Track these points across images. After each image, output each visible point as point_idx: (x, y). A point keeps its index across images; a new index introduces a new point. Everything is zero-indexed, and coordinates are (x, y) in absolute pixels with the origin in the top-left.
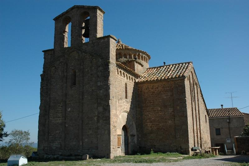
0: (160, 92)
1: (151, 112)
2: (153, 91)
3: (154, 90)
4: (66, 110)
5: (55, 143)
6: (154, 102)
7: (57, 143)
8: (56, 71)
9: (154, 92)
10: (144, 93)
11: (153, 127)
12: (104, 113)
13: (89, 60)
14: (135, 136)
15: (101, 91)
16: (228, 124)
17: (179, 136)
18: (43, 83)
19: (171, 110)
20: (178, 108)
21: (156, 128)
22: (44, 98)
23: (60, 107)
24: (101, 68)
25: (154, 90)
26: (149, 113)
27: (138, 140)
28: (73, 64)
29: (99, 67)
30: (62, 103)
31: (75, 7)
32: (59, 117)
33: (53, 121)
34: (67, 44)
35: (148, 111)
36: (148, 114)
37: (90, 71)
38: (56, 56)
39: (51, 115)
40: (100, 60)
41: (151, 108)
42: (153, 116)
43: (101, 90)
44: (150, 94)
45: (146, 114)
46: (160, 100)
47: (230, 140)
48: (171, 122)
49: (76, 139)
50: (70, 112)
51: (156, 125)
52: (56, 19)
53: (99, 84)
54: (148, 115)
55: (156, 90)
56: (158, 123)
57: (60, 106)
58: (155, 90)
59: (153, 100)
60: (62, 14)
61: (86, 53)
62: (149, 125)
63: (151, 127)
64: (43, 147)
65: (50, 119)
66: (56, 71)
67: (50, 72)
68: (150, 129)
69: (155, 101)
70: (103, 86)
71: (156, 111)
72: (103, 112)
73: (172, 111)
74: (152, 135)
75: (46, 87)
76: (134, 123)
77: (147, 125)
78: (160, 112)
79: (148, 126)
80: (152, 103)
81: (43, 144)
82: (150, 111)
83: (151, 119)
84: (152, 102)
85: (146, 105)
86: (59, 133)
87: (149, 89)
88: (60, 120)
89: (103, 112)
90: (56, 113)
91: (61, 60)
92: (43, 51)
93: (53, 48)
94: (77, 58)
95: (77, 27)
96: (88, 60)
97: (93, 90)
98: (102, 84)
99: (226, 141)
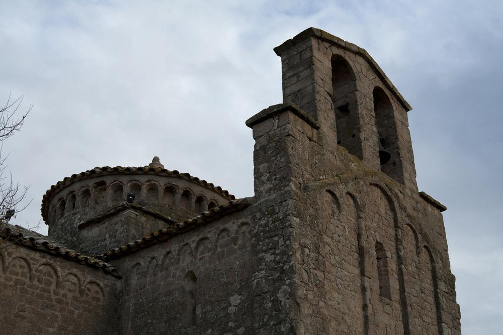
37: (417, 277)
38: (325, 157)
66: (334, 213)
75: (312, 254)
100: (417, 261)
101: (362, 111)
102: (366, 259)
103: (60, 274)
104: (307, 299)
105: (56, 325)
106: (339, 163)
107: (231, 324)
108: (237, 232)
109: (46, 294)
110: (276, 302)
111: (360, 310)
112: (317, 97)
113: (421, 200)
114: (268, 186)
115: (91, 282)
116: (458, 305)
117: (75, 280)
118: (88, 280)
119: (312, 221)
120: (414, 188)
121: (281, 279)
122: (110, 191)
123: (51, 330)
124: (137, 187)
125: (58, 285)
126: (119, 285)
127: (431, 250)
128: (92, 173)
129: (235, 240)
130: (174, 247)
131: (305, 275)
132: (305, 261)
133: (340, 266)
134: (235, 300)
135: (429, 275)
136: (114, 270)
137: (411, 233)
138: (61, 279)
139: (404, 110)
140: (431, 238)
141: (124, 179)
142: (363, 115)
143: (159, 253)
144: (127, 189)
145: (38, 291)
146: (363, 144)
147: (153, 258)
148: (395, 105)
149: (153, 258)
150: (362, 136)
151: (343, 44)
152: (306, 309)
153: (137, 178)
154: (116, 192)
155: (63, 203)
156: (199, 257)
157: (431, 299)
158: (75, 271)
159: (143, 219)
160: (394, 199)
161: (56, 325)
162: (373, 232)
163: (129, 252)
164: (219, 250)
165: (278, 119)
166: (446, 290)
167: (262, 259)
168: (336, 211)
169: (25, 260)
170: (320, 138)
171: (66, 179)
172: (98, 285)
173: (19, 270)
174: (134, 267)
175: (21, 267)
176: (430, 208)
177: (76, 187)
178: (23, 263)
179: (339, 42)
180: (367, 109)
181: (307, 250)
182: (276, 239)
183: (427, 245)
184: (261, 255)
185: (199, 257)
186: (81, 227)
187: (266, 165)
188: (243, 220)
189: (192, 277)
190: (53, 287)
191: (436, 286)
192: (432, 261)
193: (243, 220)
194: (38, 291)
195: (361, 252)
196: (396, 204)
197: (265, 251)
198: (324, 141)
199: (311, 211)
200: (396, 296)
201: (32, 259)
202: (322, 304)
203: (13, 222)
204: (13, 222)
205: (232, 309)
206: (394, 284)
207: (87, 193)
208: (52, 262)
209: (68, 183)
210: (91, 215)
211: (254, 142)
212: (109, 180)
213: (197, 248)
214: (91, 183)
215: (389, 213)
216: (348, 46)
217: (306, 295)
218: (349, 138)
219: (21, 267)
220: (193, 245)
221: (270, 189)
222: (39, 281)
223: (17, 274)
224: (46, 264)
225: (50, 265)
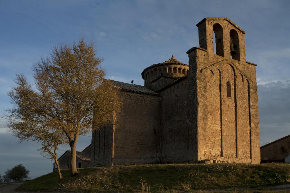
15: (253, 110)
32: (218, 124)
33: (212, 127)
37: (242, 89)
38: (209, 60)
64: (204, 152)
66: (211, 76)
75: (203, 89)
81: (204, 149)
89: (255, 128)
100: (243, 84)
101: (224, 40)
102: (222, 87)
103: (145, 98)
104: (201, 101)
105: (146, 111)
106: (215, 60)
107: (185, 108)
108: (185, 84)
109: (142, 104)
110: (194, 103)
111: (219, 102)
112: (207, 41)
113: (247, 64)
114: (192, 71)
115: (153, 99)
116: (258, 95)
117: (149, 99)
118: (152, 98)
119: (203, 80)
120: (244, 61)
121: (194, 97)
122: (158, 71)
123: (144, 112)
124: (166, 69)
125: (145, 101)
126: (161, 99)
127: (248, 80)
128: (152, 67)
129: (185, 86)
130: (172, 88)
131: (201, 95)
132: (201, 91)
134: (186, 102)
135: (247, 88)
136: (159, 95)
137: (241, 76)
138: (145, 100)
139: (243, 34)
140: (249, 76)
141: (161, 67)
142: (225, 42)
143: (169, 90)
144: (162, 70)
145: (140, 103)
146: (224, 51)
147: (168, 91)
148: (239, 33)
149: (168, 91)
150: (224, 48)
152: (200, 104)
153: (164, 66)
154: (160, 71)
155: (147, 75)
156: (178, 91)
157: (247, 95)
158: (149, 97)
159: (166, 79)
160: (234, 67)
161: (146, 111)
162: (226, 79)
163: (163, 90)
164: (182, 89)
165: (194, 52)
166: (253, 91)
167: (190, 92)
168: (212, 75)
169: (136, 96)
171: (146, 69)
172: (155, 99)
173: (135, 99)
174: (164, 93)
175: (135, 98)
176: (250, 66)
177: (149, 71)
178: (136, 97)
180: (227, 39)
181: (201, 89)
182: (193, 86)
184: (190, 90)
185: (178, 91)
186: (151, 82)
187: (191, 65)
188: (186, 81)
189: (176, 96)
190: (144, 102)
192: (249, 83)
193: (186, 81)
194: (140, 103)
195: (220, 85)
196: (235, 68)
197: (191, 90)
199: (203, 77)
200: (233, 96)
202: (206, 102)
203: (134, 83)
204: (134, 83)
205: (185, 104)
206: (232, 92)
207: (152, 72)
208: (142, 96)
209: (147, 70)
210: (154, 79)
211: (189, 58)
212: (157, 68)
213: (177, 89)
214: (153, 69)
215: (233, 71)
218: (220, 52)
219: (135, 98)
220: (176, 88)
221: (192, 72)
222: (140, 101)
223: (134, 100)
224: (141, 96)
225: (142, 96)
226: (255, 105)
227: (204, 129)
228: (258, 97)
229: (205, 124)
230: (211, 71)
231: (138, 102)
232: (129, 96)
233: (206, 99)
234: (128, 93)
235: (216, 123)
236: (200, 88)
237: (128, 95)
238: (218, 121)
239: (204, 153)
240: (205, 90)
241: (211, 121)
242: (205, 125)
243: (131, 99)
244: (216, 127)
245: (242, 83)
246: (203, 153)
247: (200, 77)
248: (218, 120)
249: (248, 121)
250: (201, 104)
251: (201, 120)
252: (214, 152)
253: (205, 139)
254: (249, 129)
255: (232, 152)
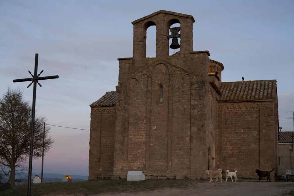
0: (244, 113)
1: (232, 134)
2: (236, 111)
3: (237, 110)
4: (150, 128)
5: (136, 163)
6: (236, 124)
7: (139, 163)
8: (136, 84)
9: (236, 113)
10: (225, 113)
11: (233, 151)
12: (199, 133)
13: (180, 76)
14: (214, 158)
15: (196, 110)
16: (289, 152)
17: (263, 161)
18: (120, 96)
19: (255, 133)
20: (264, 131)
21: (237, 151)
22: (121, 114)
23: (143, 125)
24: (195, 86)
25: (237, 110)
26: (230, 135)
27: (216, 163)
28: (159, 78)
29: (194, 84)
30: (145, 120)
31: (162, 12)
32: (141, 135)
34: (151, 53)
35: (229, 133)
36: (229, 136)
37: (181, 87)
39: (131, 133)
40: (195, 78)
41: (233, 130)
42: (234, 139)
43: (195, 109)
44: (232, 114)
45: (227, 136)
46: (245, 122)
47: (290, 171)
48: (255, 145)
49: (164, 159)
50: (155, 130)
51: (238, 148)
52: (135, 23)
53: (193, 102)
54: (229, 137)
55: (239, 111)
56: (239, 147)
57: (142, 123)
58: (238, 110)
59: (235, 122)
60: (144, 17)
61: (176, 67)
62: (229, 148)
63: (232, 150)
65: (130, 136)
67: (129, 84)
68: (231, 152)
69: (238, 122)
70: (198, 105)
71: (238, 133)
72: (198, 132)
73: (256, 135)
74: (232, 159)
76: (214, 145)
77: (227, 148)
78: (243, 135)
79: (228, 148)
80: (234, 125)
82: (231, 133)
83: (232, 141)
84: (234, 124)
85: (226, 126)
86: (142, 152)
87: (231, 109)
88: (142, 138)
89: (198, 132)
90: (138, 130)
91: (144, 72)
92: (119, 60)
93: (132, 57)
94: (164, 71)
95: (165, 37)
96: (178, 75)
97: (185, 108)
98: (196, 103)
99: (286, 172)
113: (191, 54)
127: (190, 75)
131: (120, 108)
133: (138, 99)
137: (179, 72)
151: (148, 17)
168: (137, 83)
170: (133, 62)
173: (111, 112)
175: (112, 111)
179: (146, 18)
183: (187, 74)
191: (191, 87)
198: (135, 61)
201: (114, 109)
216: (151, 16)
217: (120, 114)
223: (111, 113)
226: (199, 103)
227: (122, 143)
228: (205, 92)
229: (124, 137)
230: (135, 79)
231: (115, 115)
232: (106, 111)
233: (126, 110)
234: (104, 108)
235: (140, 134)
236: (119, 101)
237: (104, 109)
238: (142, 132)
239: (121, 168)
240: (125, 102)
241: (133, 133)
242: (123, 139)
243: (108, 113)
244: (140, 138)
245: (182, 81)
246: (120, 167)
247: (120, 90)
248: (141, 131)
249: (189, 124)
250: (119, 118)
251: (119, 134)
252: (136, 165)
253: (123, 153)
254: (189, 134)
255: (161, 164)
